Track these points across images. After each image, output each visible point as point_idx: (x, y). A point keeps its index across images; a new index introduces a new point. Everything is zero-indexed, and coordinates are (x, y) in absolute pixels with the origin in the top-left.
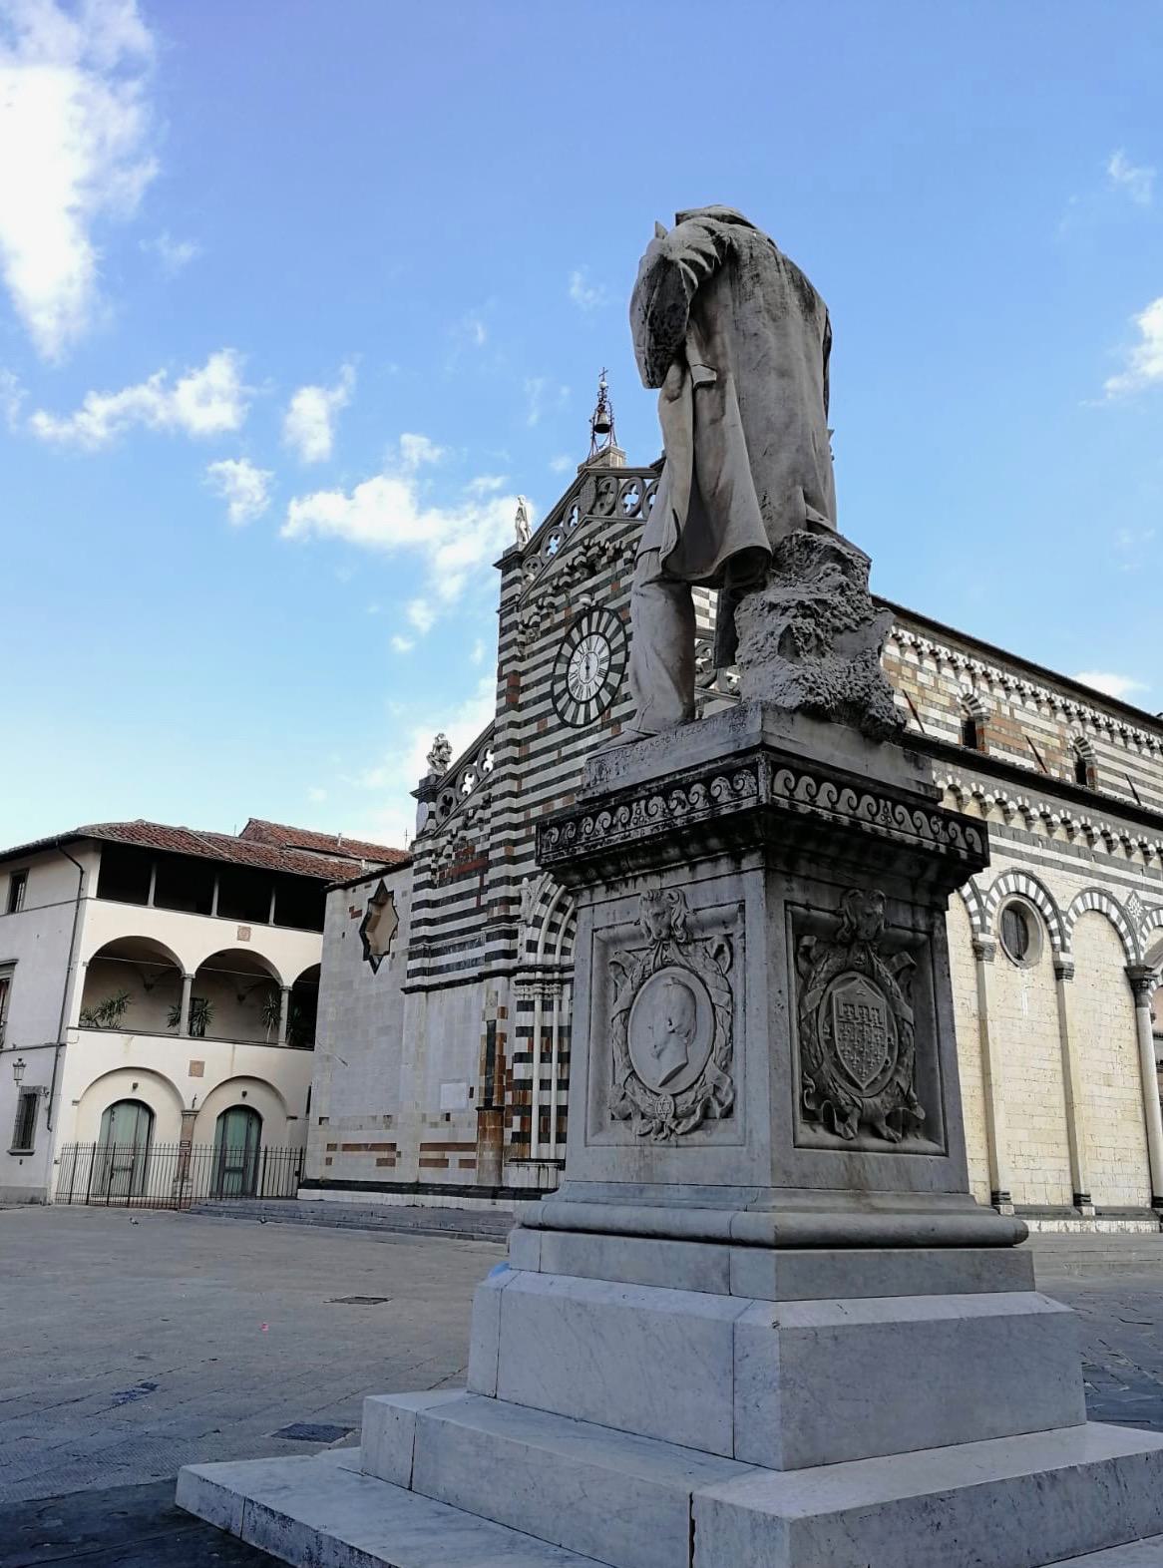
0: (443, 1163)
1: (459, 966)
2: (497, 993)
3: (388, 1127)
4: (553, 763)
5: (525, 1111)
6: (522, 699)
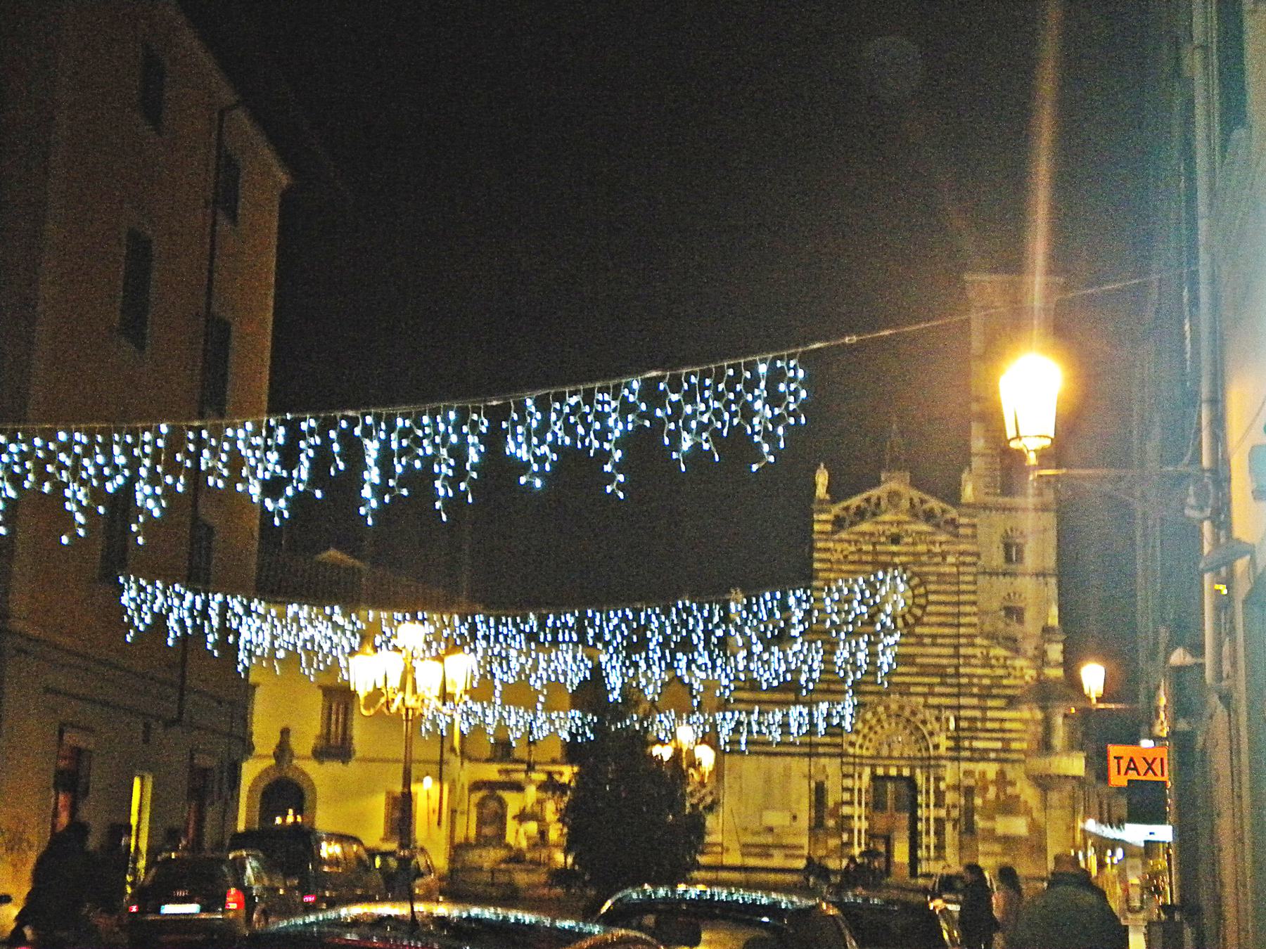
0: (768, 856)
5: (851, 831)
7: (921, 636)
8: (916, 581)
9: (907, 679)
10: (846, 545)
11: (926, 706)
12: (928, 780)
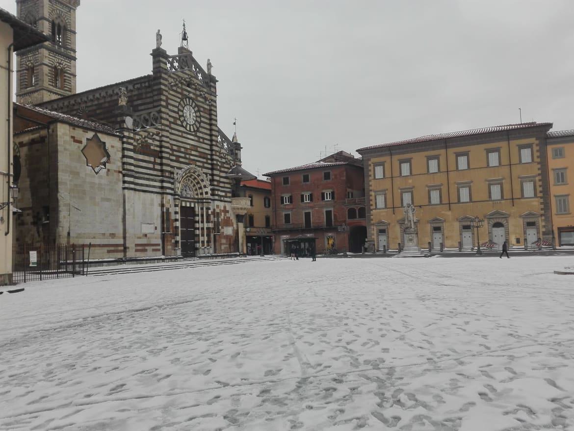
0: (145, 250)
1: (147, 186)
2: (169, 200)
3: (113, 238)
4: (177, 135)
6: (170, 107)
7: (199, 137)
8: (196, 109)
9: (199, 159)
10: (172, 80)
11: (204, 173)
12: (202, 209)
